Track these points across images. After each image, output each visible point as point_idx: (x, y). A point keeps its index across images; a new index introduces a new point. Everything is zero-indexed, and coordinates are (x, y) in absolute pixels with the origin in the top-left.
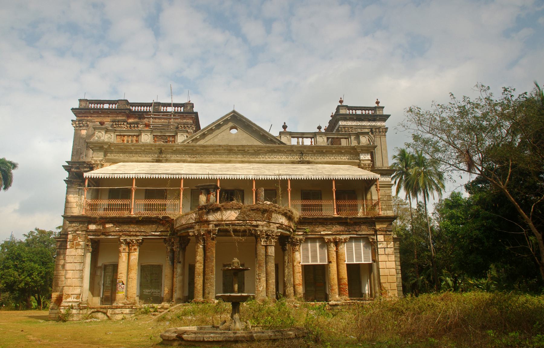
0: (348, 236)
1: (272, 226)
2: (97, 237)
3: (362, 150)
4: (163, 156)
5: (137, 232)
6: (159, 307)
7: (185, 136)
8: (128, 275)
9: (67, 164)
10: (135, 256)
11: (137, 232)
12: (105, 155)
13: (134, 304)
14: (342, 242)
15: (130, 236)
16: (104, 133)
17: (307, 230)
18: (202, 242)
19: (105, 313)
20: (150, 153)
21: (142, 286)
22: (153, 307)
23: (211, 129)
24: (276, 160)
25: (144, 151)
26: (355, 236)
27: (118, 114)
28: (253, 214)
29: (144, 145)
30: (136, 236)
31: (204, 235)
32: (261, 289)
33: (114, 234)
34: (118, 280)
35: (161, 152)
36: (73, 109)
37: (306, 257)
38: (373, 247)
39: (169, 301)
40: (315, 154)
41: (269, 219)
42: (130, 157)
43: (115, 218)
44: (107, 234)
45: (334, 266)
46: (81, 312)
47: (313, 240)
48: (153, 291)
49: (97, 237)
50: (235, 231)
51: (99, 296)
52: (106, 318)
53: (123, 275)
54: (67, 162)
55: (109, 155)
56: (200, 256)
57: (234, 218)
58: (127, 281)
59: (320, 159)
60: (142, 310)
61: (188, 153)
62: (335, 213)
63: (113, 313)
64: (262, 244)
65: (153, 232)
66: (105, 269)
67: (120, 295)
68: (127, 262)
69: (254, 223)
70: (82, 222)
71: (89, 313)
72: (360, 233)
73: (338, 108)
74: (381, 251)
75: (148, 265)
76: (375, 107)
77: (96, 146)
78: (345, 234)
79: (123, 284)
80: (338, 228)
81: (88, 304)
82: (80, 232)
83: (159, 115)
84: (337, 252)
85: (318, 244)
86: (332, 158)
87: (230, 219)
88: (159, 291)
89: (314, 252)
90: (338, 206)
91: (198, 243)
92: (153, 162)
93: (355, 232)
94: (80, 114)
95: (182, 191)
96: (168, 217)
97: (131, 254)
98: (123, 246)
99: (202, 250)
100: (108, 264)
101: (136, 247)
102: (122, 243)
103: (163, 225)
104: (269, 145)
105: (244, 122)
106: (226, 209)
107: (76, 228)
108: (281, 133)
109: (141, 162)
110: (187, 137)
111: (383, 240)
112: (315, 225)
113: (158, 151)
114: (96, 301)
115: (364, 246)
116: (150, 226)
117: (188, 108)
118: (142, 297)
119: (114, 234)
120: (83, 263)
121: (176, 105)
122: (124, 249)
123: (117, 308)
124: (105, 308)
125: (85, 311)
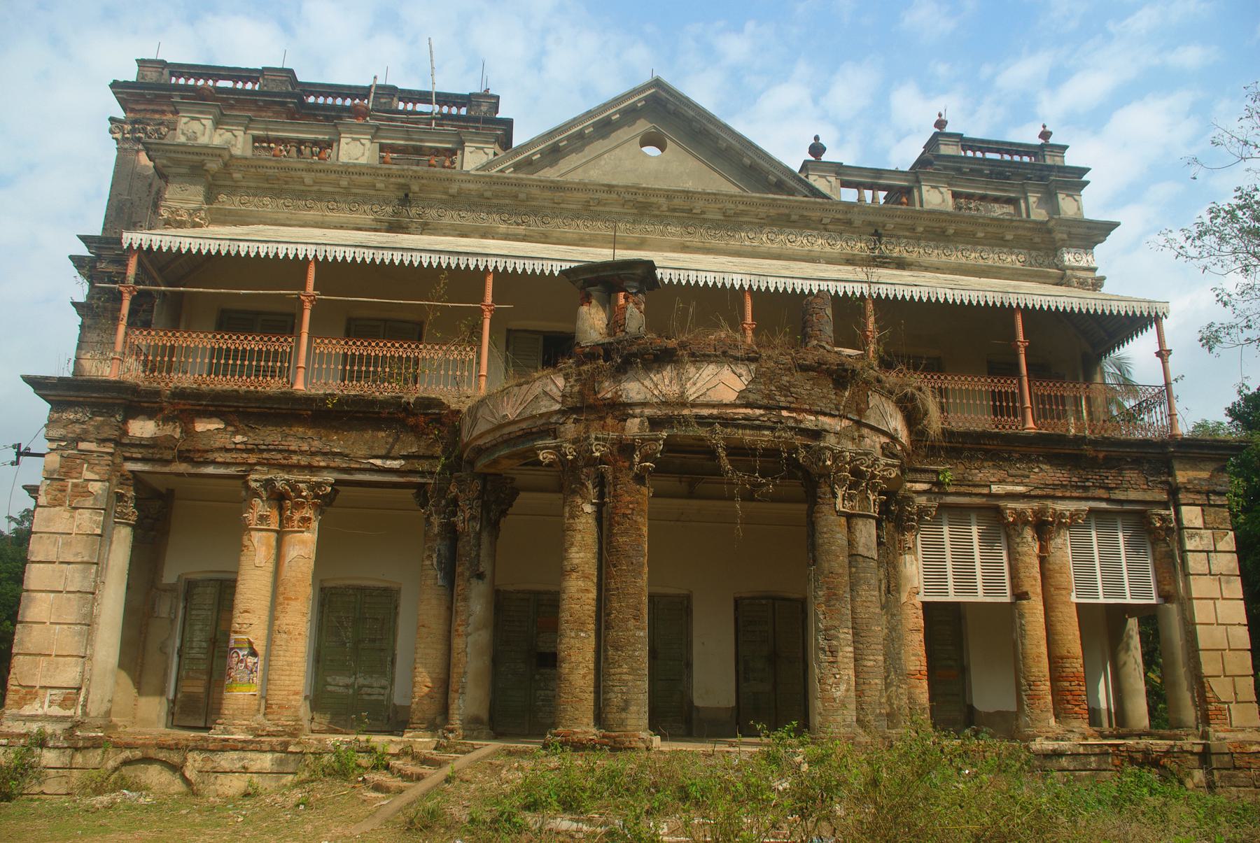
0: (1085, 506)
1: (868, 441)
2: (158, 469)
3: (1069, 234)
4: (413, 211)
5: (313, 454)
6: (394, 749)
7: (491, 152)
8: (273, 618)
9: (83, 250)
10: (303, 546)
11: (313, 454)
12: (210, 198)
13: (293, 735)
14: (1061, 525)
16: (209, 123)
17: (949, 477)
18: (592, 491)
19: (176, 769)
20: (366, 200)
21: (322, 661)
22: (370, 751)
23: (580, 135)
24: (796, 247)
26: (1104, 505)
27: (260, 109)
28: (804, 386)
30: (311, 469)
31: (601, 460)
32: (839, 692)
33: (228, 457)
34: (234, 636)
35: (406, 200)
36: (115, 85)
37: (935, 576)
39: (432, 727)
40: (919, 239)
41: (860, 412)
43: (234, 395)
44: (197, 457)
45: (1034, 609)
46: (79, 758)
47: (959, 514)
48: (361, 681)
49: (158, 469)
50: (738, 451)
51: (162, 692)
52: (178, 786)
53: (255, 621)
55: (223, 197)
57: (730, 397)
58: (270, 641)
59: (935, 256)
60: (326, 757)
61: (500, 209)
62: (1030, 424)
63: (208, 768)
64: (839, 506)
65: (379, 456)
66: (188, 596)
67: (241, 695)
68: (270, 567)
69: (809, 421)
70: (99, 408)
71: (111, 764)
72: (1119, 495)
74: (1196, 563)
75: (348, 587)
76: (1041, 147)
77: (178, 163)
78: (1071, 498)
79: (254, 653)
80: (1046, 474)
81: (109, 726)
82: (92, 446)
83: (392, 120)
84: (1042, 560)
85: (975, 531)
86: (973, 257)
87: (714, 397)
88: (384, 682)
89: (964, 556)
90: (1038, 399)
91: (574, 492)
92: (376, 230)
93: (1102, 493)
94: (137, 102)
95: (488, 315)
96: (438, 403)
97: (288, 538)
98: (260, 507)
99: (591, 521)
100: (199, 577)
101: (308, 512)
102: (256, 494)
103: (417, 431)
106: (700, 358)
107: (77, 428)
108: (805, 166)
109: (336, 228)
110: (495, 154)
111: (1199, 523)
112: (970, 459)
114: (149, 717)
115: (1128, 544)
116: (368, 435)
117: (484, 108)
118: (318, 700)
119: (228, 457)
120: (98, 564)
121: (444, 99)
122: (262, 518)
124: (176, 747)
125: (95, 757)
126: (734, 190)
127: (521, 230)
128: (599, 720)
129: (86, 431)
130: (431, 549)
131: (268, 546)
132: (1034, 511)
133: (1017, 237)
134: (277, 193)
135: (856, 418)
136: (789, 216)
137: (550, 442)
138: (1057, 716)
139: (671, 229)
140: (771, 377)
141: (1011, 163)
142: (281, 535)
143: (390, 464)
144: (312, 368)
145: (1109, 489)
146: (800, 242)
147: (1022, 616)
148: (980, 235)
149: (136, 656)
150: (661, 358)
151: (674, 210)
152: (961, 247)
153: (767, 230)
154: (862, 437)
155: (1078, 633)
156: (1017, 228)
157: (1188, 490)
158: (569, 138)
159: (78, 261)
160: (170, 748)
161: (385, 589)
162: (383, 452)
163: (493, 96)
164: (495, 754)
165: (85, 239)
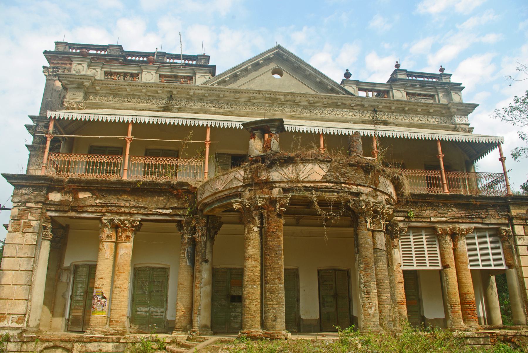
0: (473, 226)
3: (457, 109)
4: (174, 103)
5: (131, 207)
6: (168, 340)
7: (207, 77)
8: (113, 281)
9: (31, 122)
10: (127, 249)
11: (131, 207)
12: (86, 97)
13: (122, 334)
14: (462, 235)
15: (120, 214)
16: (86, 66)
17: (412, 214)
18: (258, 222)
20: (154, 98)
22: (157, 341)
23: (246, 70)
24: (340, 117)
25: (145, 95)
26: (480, 226)
28: (351, 173)
29: (145, 85)
30: (130, 214)
31: (262, 207)
32: (372, 311)
33: (93, 209)
34: (95, 290)
35: (171, 98)
36: (45, 53)
37: (407, 258)
38: (507, 244)
39: (185, 330)
40: (393, 112)
41: (376, 185)
42: (124, 102)
43: (96, 182)
45: (452, 272)
46: (25, 347)
47: (417, 230)
48: (152, 309)
50: (323, 203)
51: (63, 315)
53: (105, 283)
54: (31, 117)
55: (91, 98)
56: (254, 247)
57: (319, 178)
58: (112, 292)
59: (400, 119)
60: (138, 345)
61: (211, 101)
62: (446, 190)
63: (83, 350)
65: (161, 208)
66: (75, 272)
67: (98, 316)
68: (112, 258)
69: (354, 189)
70: (36, 188)
71: (39, 349)
72: (487, 221)
73: (395, 73)
75: (146, 267)
76: (440, 75)
78: (466, 223)
79: (104, 298)
80: (454, 212)
81: (39, 332)
82: (33, 205)
84: (455, 250)
85: (424, 238)
86: (416, 120)
87: (311, 178)
88: (162, 310)
89: (420, 249)
90: (448, 180)
91: (249, 222)
92: (158, 111)
93: (479, 220)
94: (54, 60)
96: (187, 184)
97: (120, 245)
98: (107, 231)
99: (258, 235)
100: (80, 263)
101: (129, 234)
102: (106, 226)
103: (178, 197)
104: (330, 94)
105: (293, 63)
106: (305, 161)
108: (343, 82)
109: (140, 110)
110: (209, 78)
111: (522, 233)
113: (166, 95)
114: (58, 327)
115: (491, 243)
116: (155, 199)
118: (133, 319)
119: (93, 209)
120: (35, 258)
121: (186, 57)
122: (108, 236)
123: (92, 340)
124: (69, 341)
126: (313, 93)
127: (221, 110)
128: (263, 326)
129: (30, 198)
130: (184, 249)
131: (111, 248)
132: (450, 229)
133: (435, 111)
134: (115, 95)
135: (374, 187)
136: (337, 103)
137: (238, 200)
138: (464, 320)
139: (286, 109)
140: (337, 169)
141: (428, 82)
142: (117, 244)
143: (165, 211)
144: (131, 170)
145: (482, 218)
146: (342, 114)
147: (447, 275)
148: (419, 110)
149: (51, 299)
150: (289, 161)
151: (287, 101)
152: (411, 116)
153: (327, 109)
154: (377, 195)
155: (472, 283)
156: (434, 107)
157: (517, 219)
158: (241, 71)
159: (28, 127)
160: (66, 341)
161: (163, 268)
162: (162, 206)
163: (207, 56)
164: (215, 342)
165: (31, 117)
